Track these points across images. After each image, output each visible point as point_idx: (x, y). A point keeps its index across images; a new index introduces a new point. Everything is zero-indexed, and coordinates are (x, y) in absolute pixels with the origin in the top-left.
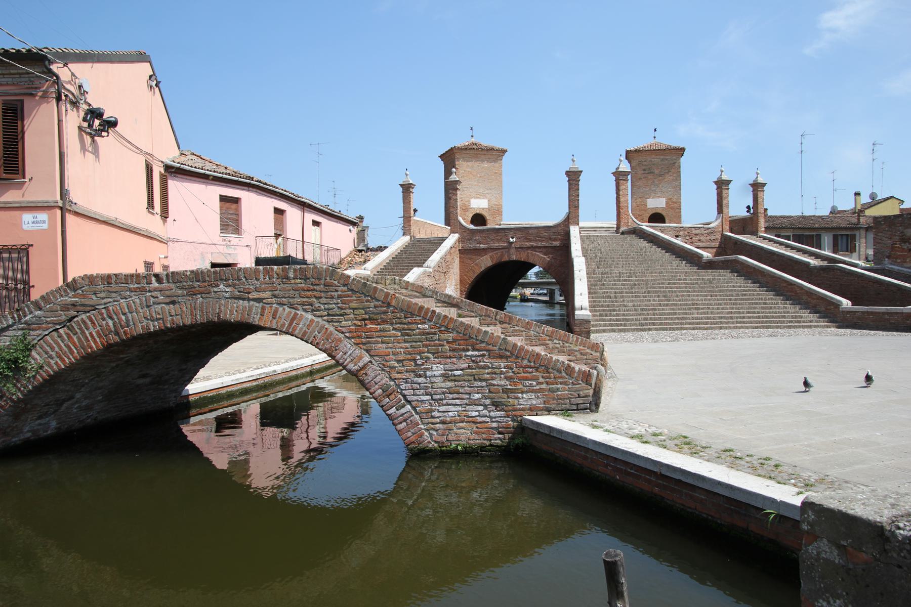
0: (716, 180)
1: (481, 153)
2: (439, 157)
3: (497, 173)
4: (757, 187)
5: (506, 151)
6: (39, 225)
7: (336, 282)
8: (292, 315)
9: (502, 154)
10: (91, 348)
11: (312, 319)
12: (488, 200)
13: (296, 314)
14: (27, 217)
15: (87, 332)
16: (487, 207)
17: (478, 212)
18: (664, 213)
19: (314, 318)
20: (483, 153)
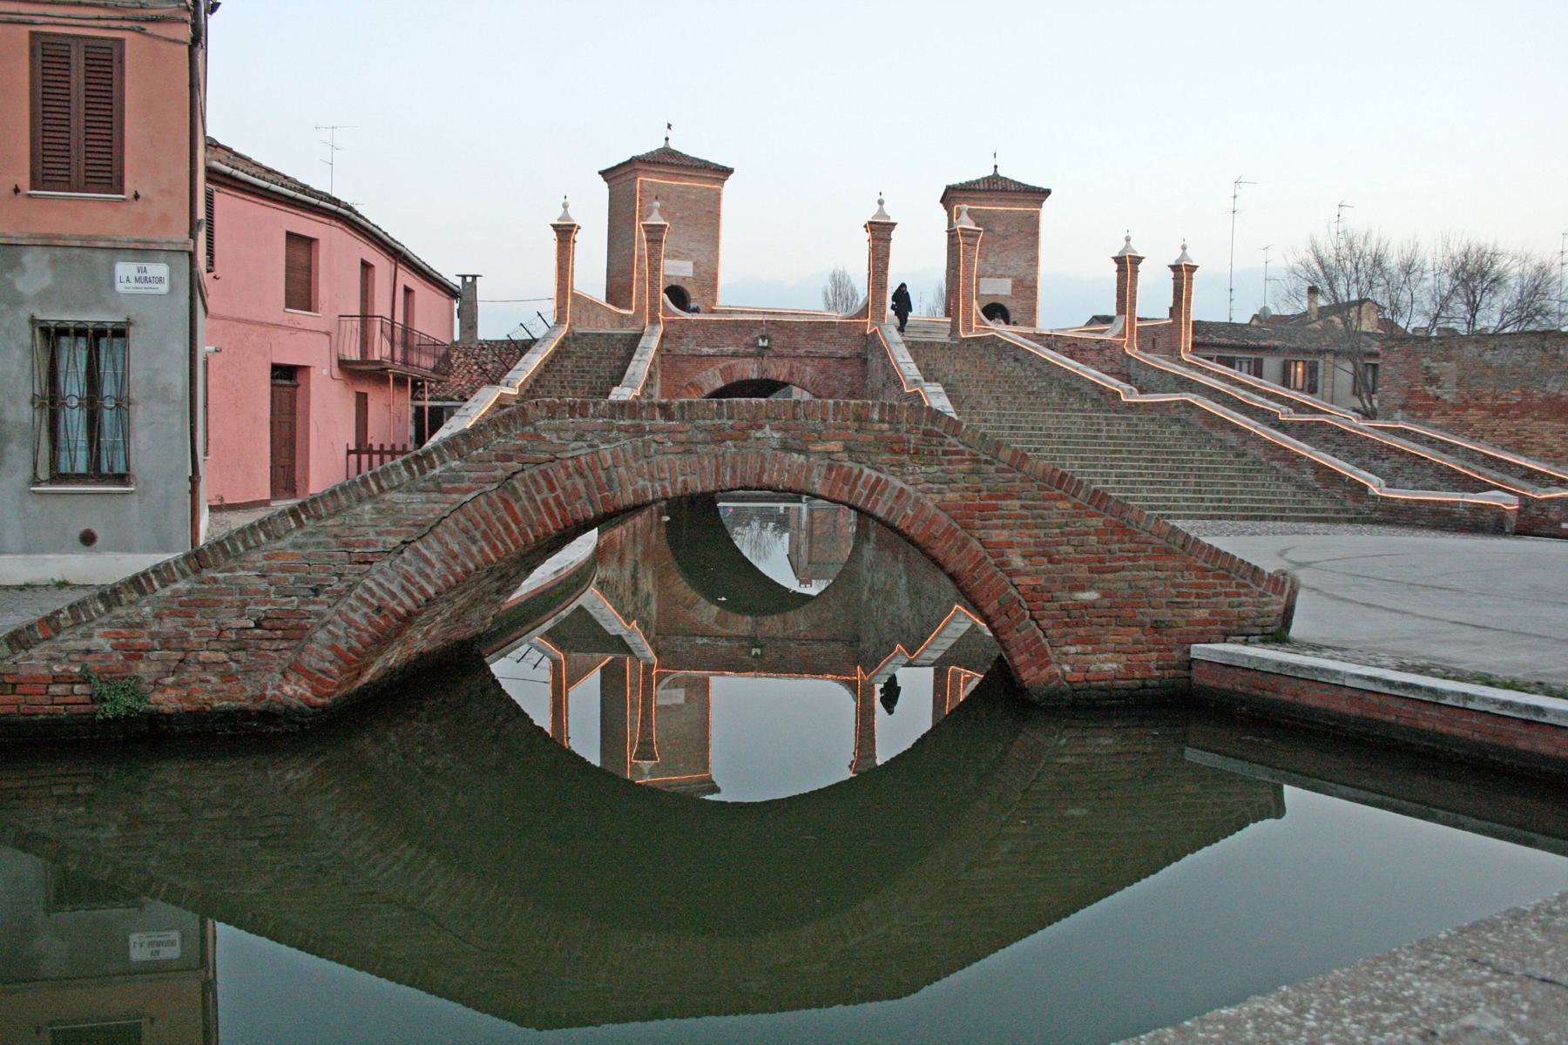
0: (1117, 255)
1: (685, 173)
2: (600, 173)
3: (710, 212)
4: (1182, 273)
5: (727, 172)
6: (150, 285)
7: (941, 431)
8: (873, 480)
9: (722, 177)
10: (546, 526)
11: (902, 488)
12: (694, 264)
13: (878, 480)
14: (125, 270)
15: (538, 498)
16: (691, 275)
17: (675, 284)
18: (1009, 305)
19: (904, 486)
20: (689, 173)
